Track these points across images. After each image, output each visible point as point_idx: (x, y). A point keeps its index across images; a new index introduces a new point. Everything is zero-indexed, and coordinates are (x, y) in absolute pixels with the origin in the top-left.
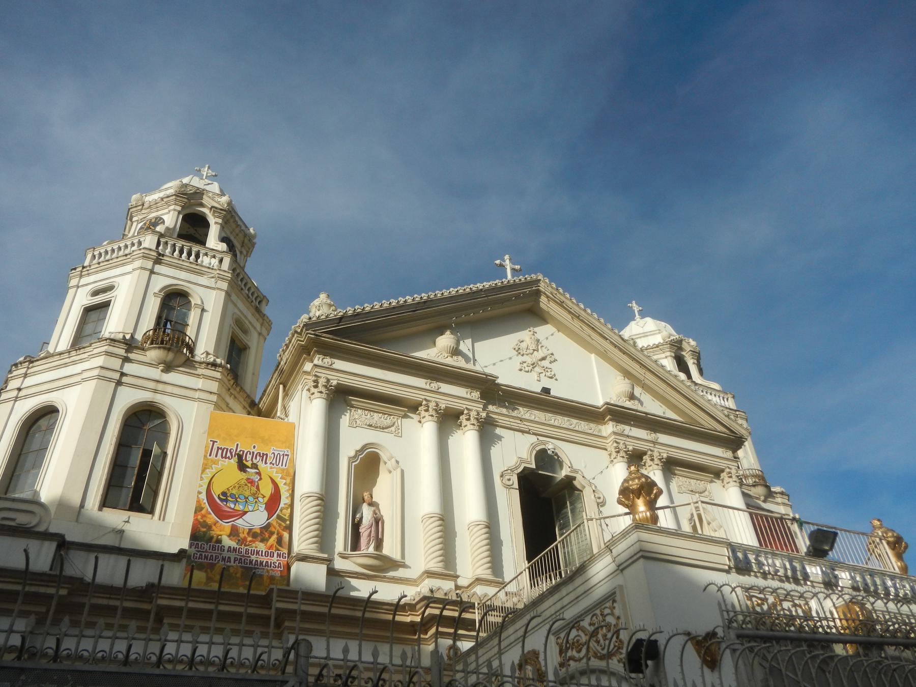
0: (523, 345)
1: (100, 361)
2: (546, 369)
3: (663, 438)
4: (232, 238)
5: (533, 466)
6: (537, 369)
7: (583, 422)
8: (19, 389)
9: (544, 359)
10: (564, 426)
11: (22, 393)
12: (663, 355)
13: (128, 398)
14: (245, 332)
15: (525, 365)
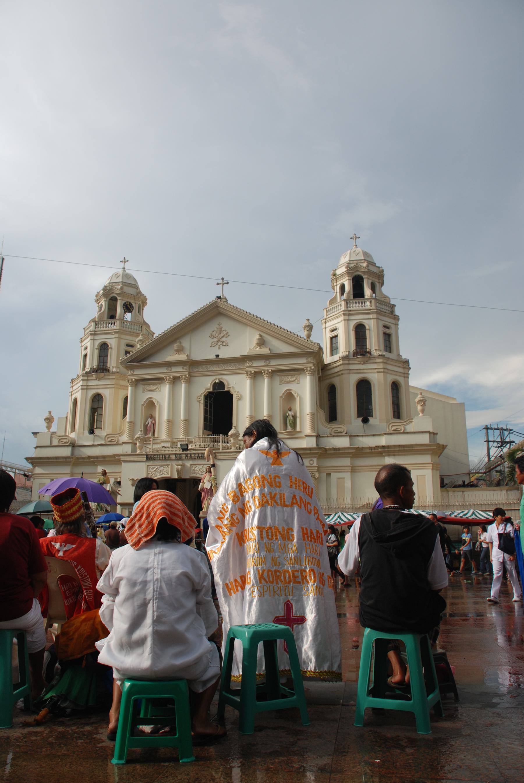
0: (214, 333)
1: (81, 384)
2: (223, 342)
3: (273, 362)
4: (129, 300)
5: (211, 390)
6: (219, 344)
7: (236, 364)
8: (72, 392)
9: (223, 337)
10: (227, 369)
11: (73, 393)
12: (345, 280)
13: (91, 393)
14: (132, 346)
15: (213, 343)
